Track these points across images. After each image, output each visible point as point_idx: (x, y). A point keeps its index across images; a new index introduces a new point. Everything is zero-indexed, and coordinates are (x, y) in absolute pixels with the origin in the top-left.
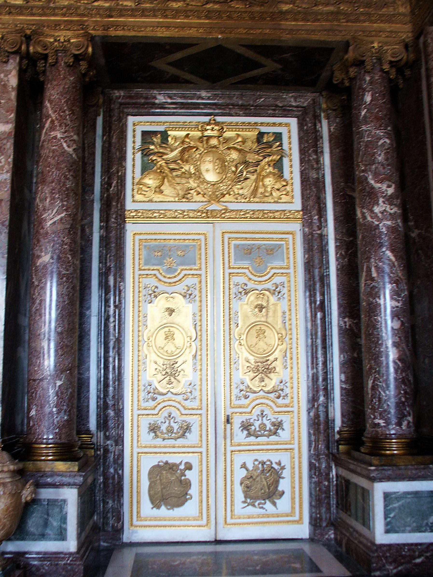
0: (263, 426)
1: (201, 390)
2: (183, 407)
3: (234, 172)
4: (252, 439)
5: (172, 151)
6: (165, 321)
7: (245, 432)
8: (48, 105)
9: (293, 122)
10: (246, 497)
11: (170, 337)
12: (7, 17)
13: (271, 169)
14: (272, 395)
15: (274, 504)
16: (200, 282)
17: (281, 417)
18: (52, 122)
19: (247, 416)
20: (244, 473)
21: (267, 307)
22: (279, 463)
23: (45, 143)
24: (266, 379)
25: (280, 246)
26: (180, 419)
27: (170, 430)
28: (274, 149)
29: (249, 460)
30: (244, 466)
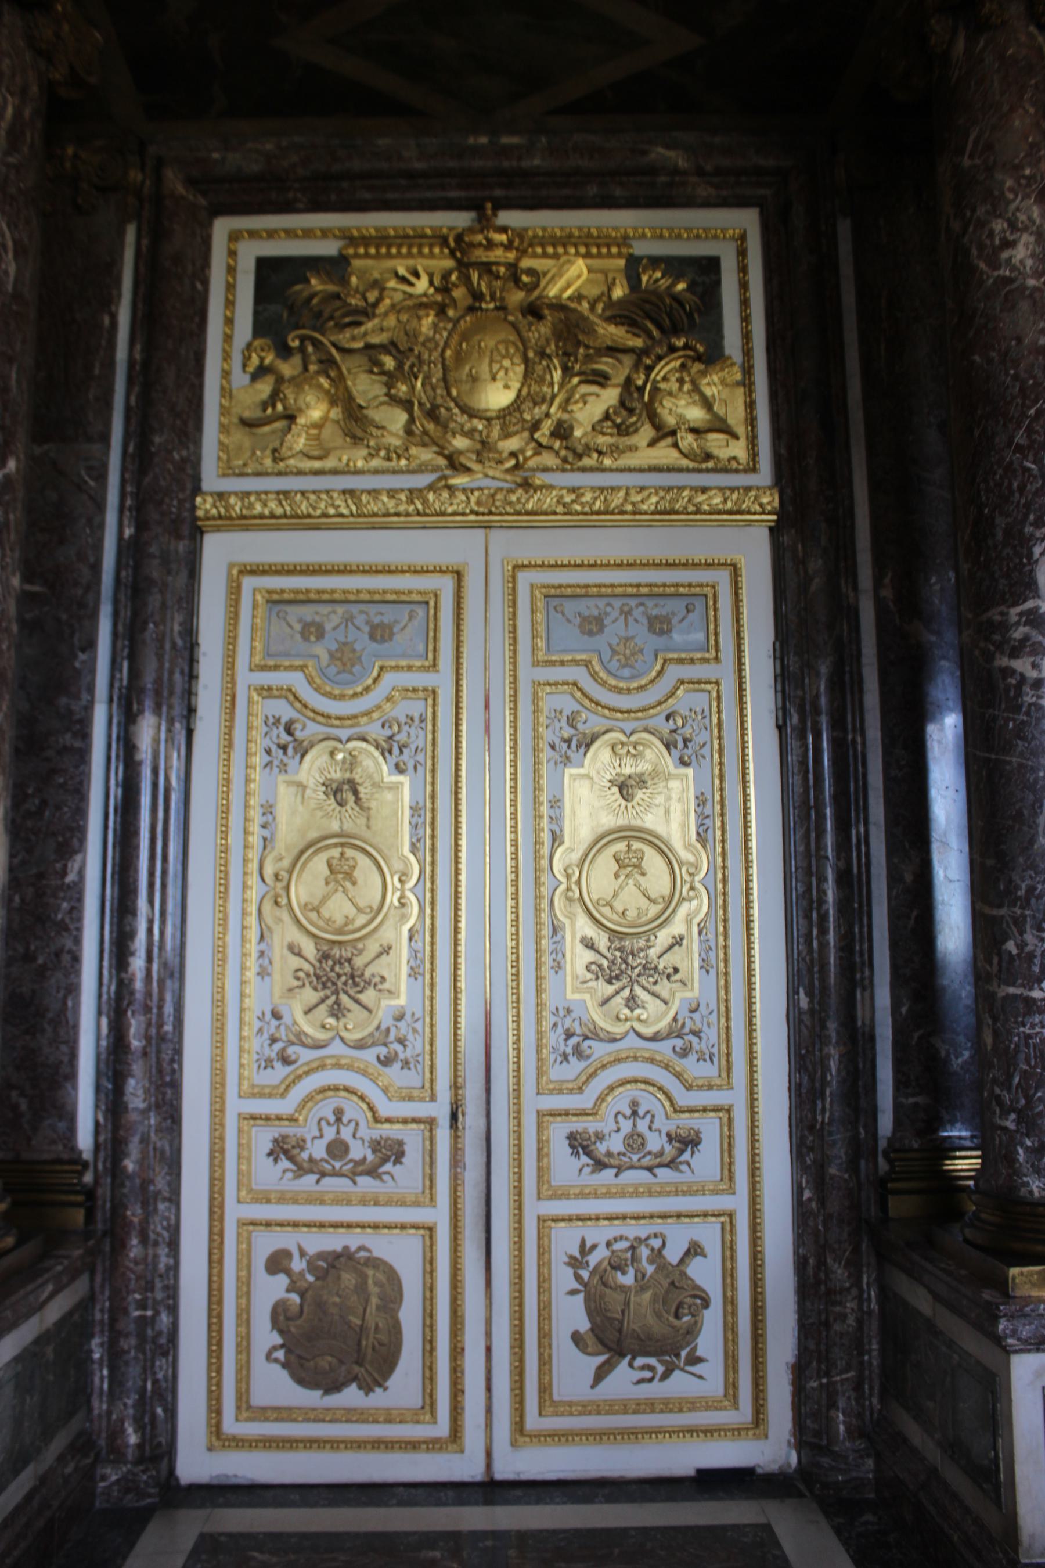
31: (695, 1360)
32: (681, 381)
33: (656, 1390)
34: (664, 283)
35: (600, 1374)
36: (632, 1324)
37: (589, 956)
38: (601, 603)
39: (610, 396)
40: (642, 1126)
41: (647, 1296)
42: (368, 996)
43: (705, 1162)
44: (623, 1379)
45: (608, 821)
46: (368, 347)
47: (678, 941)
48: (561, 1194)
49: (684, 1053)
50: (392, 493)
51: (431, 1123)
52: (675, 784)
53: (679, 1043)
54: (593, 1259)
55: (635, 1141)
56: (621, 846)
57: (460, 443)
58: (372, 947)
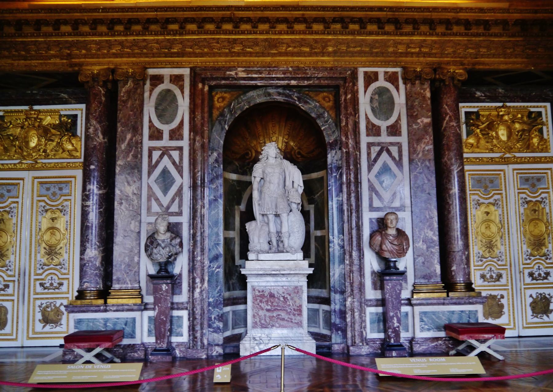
0: (540, 275)
1: (506, 255)
2: (498, 264)
3: (517, 135)
4: (534, 281)
5: (483, 124)
6: (485, 219)
7: (531, 278)
8: (446, 107)
9: (548, 105)
10: (533, 313)
11: (488, 227)
12: (422, 58)
13: (537, 133)
14: (543, 258)
15: (548, 316)
16: (502, 197)
17: (549, 270)
18: (450, 117)
19: (532, 270)
20: (531, 300)
21: (538, 211)
22: (549, 295)
23: (448, 129)
24: (540, 250)
25: (544, 177)
26: (495, 271)
27: (491, 277)
28: (538, 121)
29: (534, 292)
30: (531, 296)
31: (61, 325)
32: (67, 141)
33: (54, 330)
34: (66, 120)
35: (44, 327)
36: (50, 318)
37: (45, 251)
38: (50, 185)
39: (55, 144)
40: (53, 282)
41: (53, 313)
42: (4, 258)
43: (64, 288)
44: (48, 328)
45: (50, 226)
46: (8, 135)
47: (61, 248)
48: (37, 294)
49: (61, 268)
50: (11, 164)
51: (14, 281)
52: (62, 219)
53: (60, 266)
54: (43, 306)
55: (52, 284)
56: (51, 230)
57: (25, 153)
58: (5, 249)
